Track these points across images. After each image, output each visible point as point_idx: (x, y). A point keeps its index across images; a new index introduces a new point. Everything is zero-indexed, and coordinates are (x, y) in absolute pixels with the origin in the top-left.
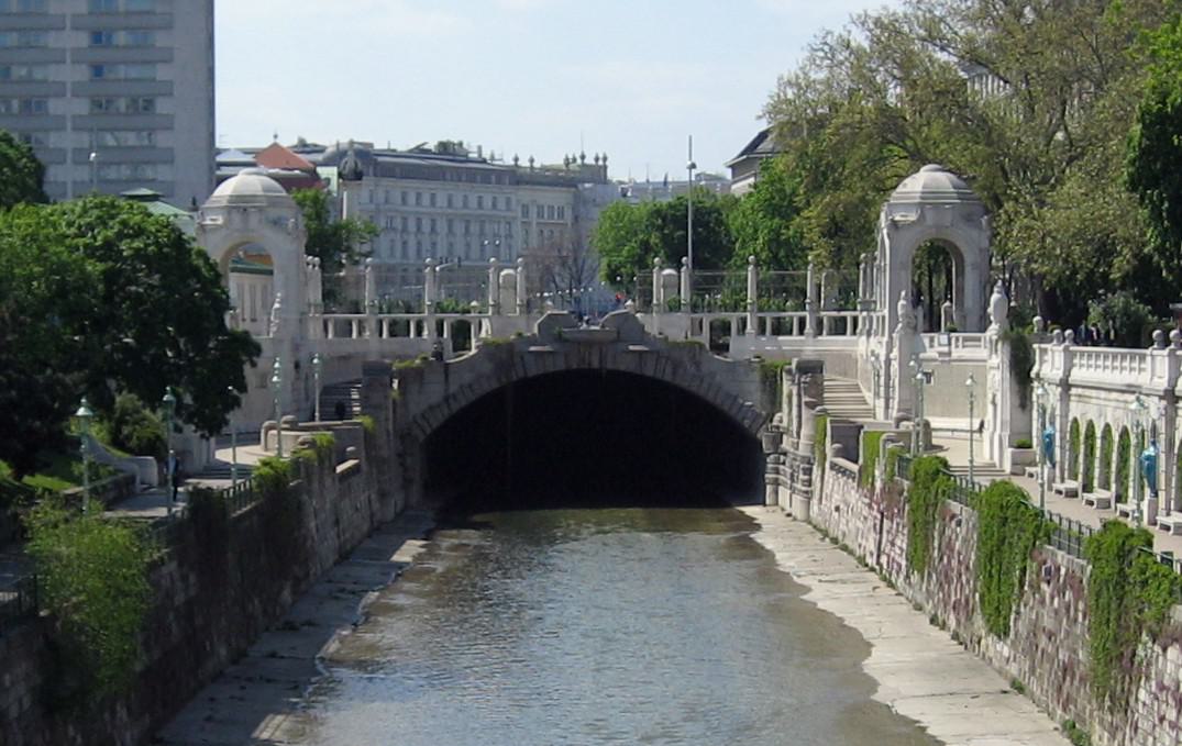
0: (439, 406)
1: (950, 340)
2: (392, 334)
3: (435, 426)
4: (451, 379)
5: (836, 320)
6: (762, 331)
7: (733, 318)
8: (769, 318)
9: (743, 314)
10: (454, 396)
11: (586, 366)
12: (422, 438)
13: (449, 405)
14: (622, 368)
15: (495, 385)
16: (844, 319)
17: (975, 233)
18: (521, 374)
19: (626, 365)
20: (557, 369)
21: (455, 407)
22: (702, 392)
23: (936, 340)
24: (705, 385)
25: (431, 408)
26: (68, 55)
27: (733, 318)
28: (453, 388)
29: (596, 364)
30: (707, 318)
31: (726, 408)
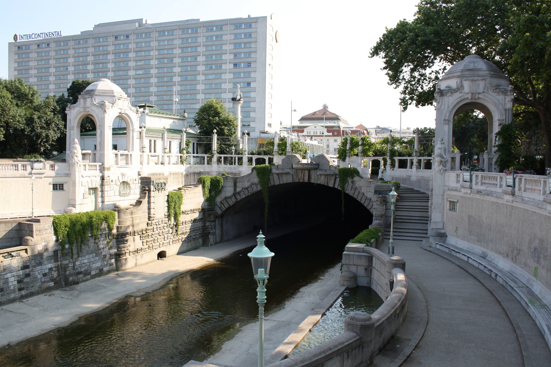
0: (230, 197)
1: (471, 176)
3: (227, 206)
4: (238, 184)
5: (400, 161)
7: (380, 159)
10: (239, 193)
12: (219, 212)
13: (235, 197)
14: (319, 182)
15: (259, 188)
17: (501, 97)
18: (272, 184)
19: (322, 181)
20: (289, 182)
21: (239, 198)
22: (355, 196)
23: (461, 176)
24: (357, 193)
25: (226, 198)
27: (380, 159)
28: (238, 190)
29: (306, 180)
31: (365, 205)
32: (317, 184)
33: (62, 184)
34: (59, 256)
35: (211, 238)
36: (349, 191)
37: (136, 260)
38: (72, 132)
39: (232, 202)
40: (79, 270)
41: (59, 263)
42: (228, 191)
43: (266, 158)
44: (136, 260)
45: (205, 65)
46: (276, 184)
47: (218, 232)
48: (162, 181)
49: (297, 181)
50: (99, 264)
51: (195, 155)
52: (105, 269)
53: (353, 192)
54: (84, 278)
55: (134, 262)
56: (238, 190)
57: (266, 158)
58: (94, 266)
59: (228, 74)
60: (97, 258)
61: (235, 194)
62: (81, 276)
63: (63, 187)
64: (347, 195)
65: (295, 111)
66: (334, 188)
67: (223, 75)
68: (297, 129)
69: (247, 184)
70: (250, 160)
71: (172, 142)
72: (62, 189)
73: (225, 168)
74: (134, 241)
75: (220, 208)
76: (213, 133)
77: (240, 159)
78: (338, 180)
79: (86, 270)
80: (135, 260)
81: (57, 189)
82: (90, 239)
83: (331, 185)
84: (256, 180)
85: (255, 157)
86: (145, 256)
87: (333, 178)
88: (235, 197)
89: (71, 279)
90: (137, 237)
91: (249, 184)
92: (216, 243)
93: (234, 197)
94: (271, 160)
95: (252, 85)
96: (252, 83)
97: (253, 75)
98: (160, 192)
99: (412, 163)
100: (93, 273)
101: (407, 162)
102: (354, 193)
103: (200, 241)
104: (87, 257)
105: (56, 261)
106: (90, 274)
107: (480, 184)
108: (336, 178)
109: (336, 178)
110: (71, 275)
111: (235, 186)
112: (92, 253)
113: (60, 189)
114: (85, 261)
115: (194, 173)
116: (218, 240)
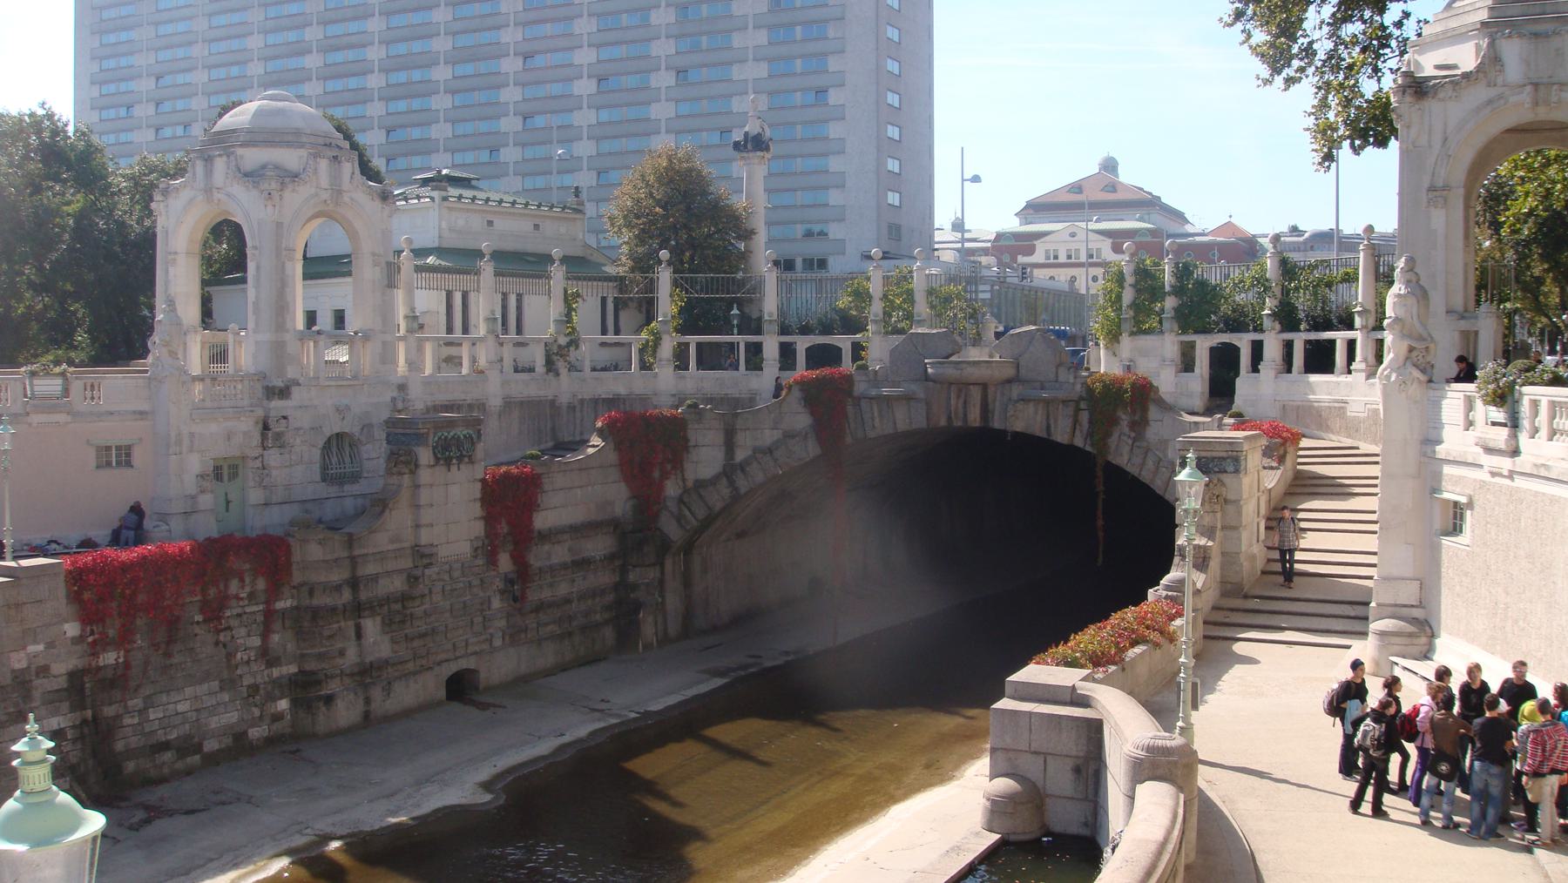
0: (714, 481)
2: (701, 364)
3: (701, 513)
6: (1288, 365)
8: (1299, 339)
9: (1257, 337)
10: (742, 467)
11: (960, 424)
13: (731, 483)
14: (1019, 426)
16: (1332, 343)
20: (914, 427)
24: (1150, 464)
25: (700, 484)
26: (750, 85)
28: (740, 455)
29: (975, 418)
30: (1204, 345)
32: (1016, 434)
33: (129, 447)
34: (88, 692)
35: (649, 628)
36: (1123, 455)
37: (368, 701)
38: (171, 270)
39: (718, 497)
40: (161, 736)
41: (89, 713)
42: (705, 460)
43: (843, 342)
44: (368, 701)
45: (676, 37)
46: (871, 434)
47: (673, 601)
48: (461, 432)
49: (943, 422)
50: (231, 717)
51: (611, 337)
52: (255, 733)
53: (1137, 460)
54: (179, 765)
55: (359, 708)
56: (740, 455)
57: (843, 342)
58: (215, 722)
59: (750, 63)
60: (226, 697)
61: (730, 470)
62: (168, 756)
63: (128, 455)
64: (1117, 474)
65: (976, 179)
66: (1071, 448)
67: (735, 68)
68: (1013, 243)
69: (769, 436)
70: (787, 352)
71: (526, 299)
72: (129, 464)
73: (699, 381)
74: (359, 635)
75: (679, 519)
76: (660, 262)
77: (755, 350)
78: (1084, 417)
79: (189, 737)
80: (361, 701)
81: (109, 464)
82: (197, 630)
83: (1061, 435)
84: (801, 420)
85: (802, 344)
86: (398, 687)
87: (1070, 410)
88: (731, 483)
89: (130, 766)
90: (371, 626)
91: (777, 434)
92: (665, 640)
93: (724, 481)
94: (857, 349)
95: (834, 97)
96: (832, 92)
97: (833, 64)
98: (454, 468)
99: (1351, 357)
100: (210, 745)
101: (747, 362)
102: (1143, 464)
103: (609, 633)
104: (189, 691)
105: (78, 705)
106: (198, 749)
107: (1544, 432)
108: (1078, 410)
109: (1078, 410)
110: (130, 753)
111: (730, 446)
112: (206, 677)
113: (119, 464)
114: (181, 708)
115: (596, 401)
116: (673, 630)
